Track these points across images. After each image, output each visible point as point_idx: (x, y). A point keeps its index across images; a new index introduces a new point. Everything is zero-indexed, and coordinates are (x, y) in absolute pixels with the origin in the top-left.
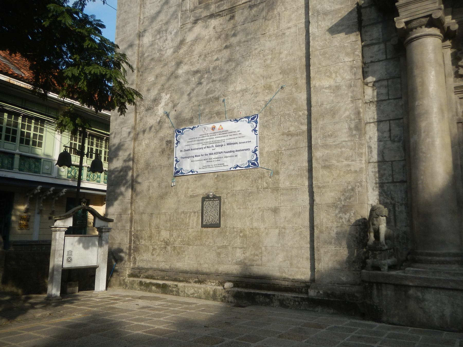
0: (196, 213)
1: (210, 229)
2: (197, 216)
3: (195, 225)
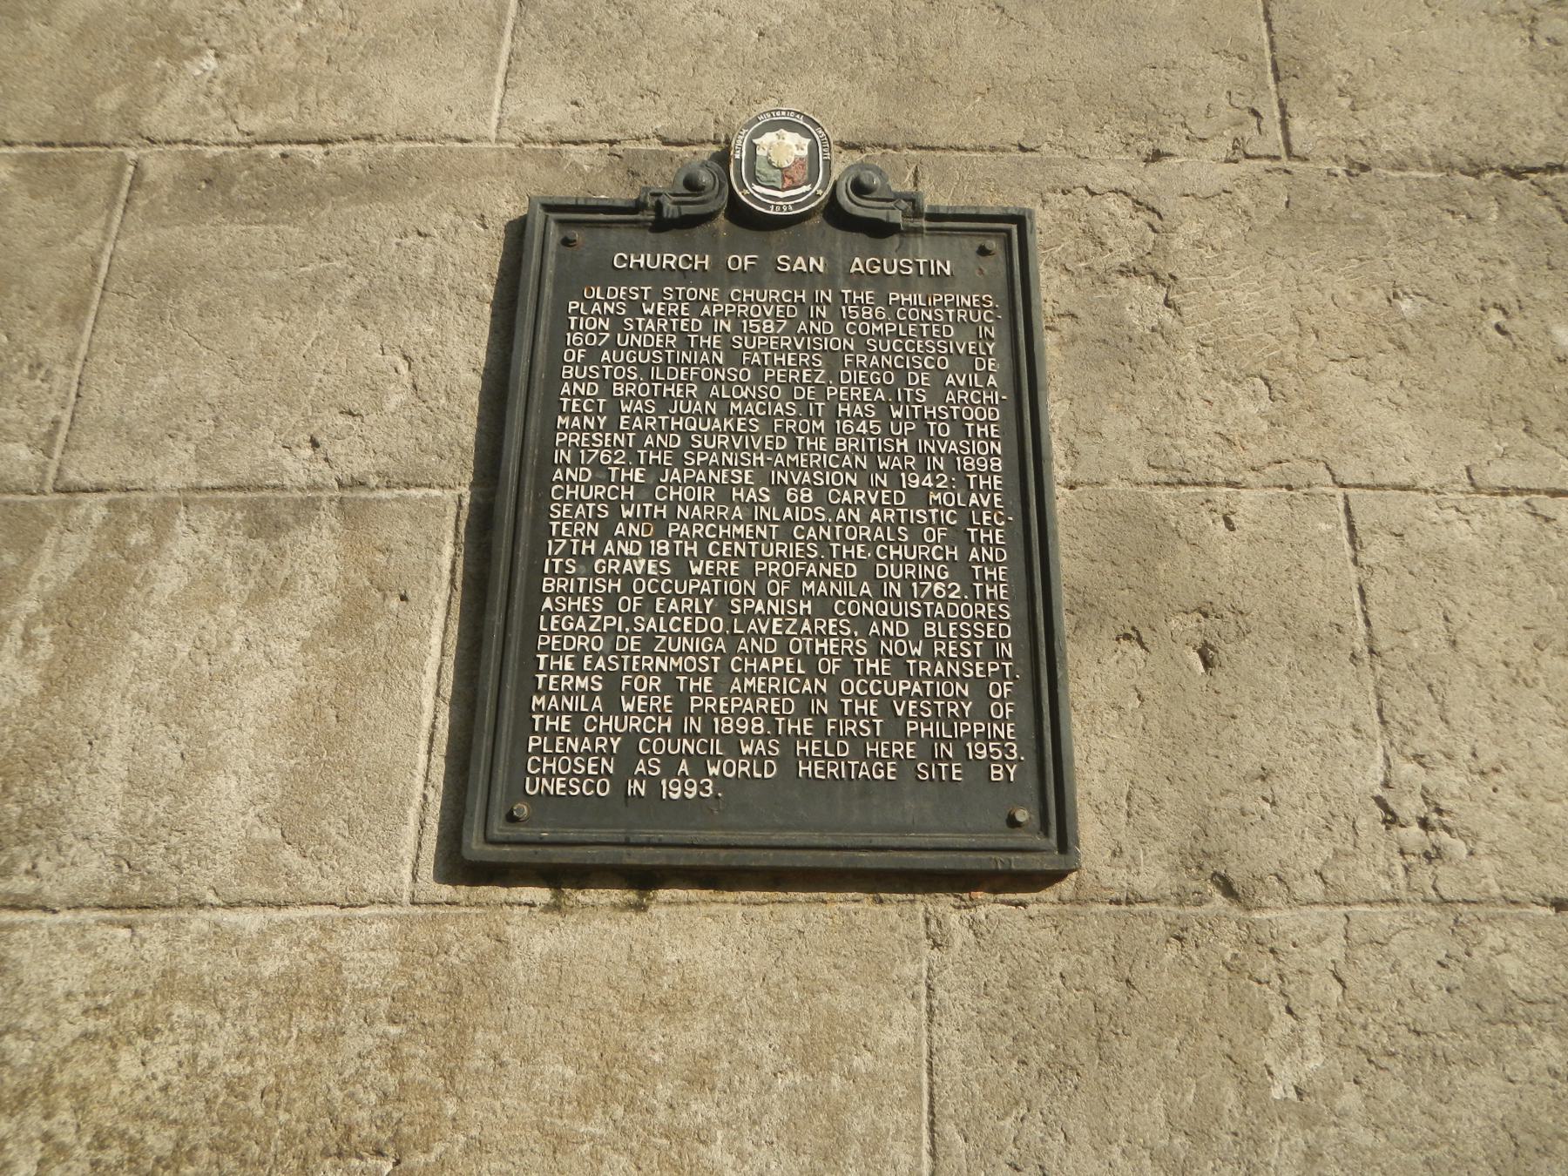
0: (319, 548)
1: (703, 935)
2: (314, 602)
3: (231, 806)
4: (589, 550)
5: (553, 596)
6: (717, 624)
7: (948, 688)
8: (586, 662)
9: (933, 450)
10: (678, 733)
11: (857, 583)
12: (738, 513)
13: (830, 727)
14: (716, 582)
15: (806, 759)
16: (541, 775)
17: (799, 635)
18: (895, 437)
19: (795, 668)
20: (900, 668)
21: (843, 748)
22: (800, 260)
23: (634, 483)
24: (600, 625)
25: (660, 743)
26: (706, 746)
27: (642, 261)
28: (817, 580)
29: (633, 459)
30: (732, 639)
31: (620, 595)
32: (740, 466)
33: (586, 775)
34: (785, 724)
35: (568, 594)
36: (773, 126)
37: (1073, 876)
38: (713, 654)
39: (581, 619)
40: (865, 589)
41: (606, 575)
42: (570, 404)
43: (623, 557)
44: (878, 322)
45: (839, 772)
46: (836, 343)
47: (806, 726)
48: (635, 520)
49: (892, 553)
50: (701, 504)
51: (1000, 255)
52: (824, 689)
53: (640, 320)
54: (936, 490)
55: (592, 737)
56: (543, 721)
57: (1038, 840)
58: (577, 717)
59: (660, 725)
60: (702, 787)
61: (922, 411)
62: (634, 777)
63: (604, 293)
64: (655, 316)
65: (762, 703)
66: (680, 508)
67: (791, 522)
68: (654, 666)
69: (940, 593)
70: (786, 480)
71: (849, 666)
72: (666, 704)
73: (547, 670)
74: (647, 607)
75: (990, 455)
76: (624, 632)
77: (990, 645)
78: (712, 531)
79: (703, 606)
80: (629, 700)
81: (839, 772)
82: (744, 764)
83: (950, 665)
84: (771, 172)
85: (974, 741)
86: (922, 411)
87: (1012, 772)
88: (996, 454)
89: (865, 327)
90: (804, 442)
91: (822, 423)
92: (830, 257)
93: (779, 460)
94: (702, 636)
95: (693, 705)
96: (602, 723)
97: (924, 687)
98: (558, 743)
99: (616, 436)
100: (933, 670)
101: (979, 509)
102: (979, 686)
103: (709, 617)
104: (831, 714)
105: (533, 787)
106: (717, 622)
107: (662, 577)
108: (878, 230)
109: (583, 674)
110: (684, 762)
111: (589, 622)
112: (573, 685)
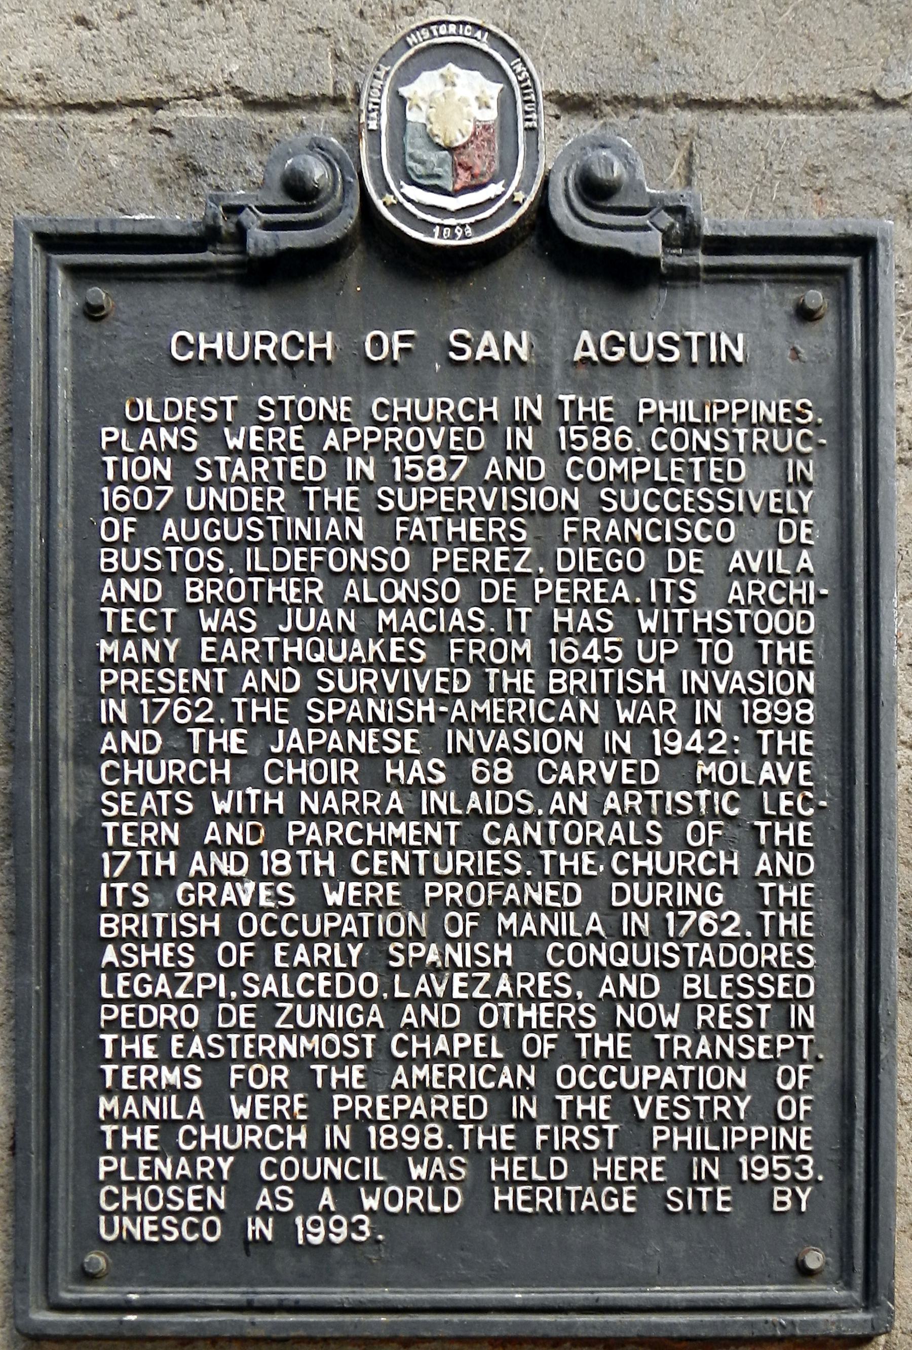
4: (166, 868)
5: (117, 941)
8: (175, 1045)
9: (705, 688)
10: (317, 1149)
12: (396, 802)
13: (540, 1138)
14: (366, 916)
15: (505, 1183)
17: (494, 1000)
18: (643, 666)
19: (486, 1049)
20: (645, 1046)
21: (559, 1167)
22: (488, 337)
24: (192, 987)
25: (290, 1165)
26: (357, 1168)
27: (218, 346)
28: (521, 911)
29: (224, 715)
30: (393, 1006)
31: (219, 940)
33: (185, 1212)
34: (473, 1133)
35: (139, 940)
37: (882, 1339)
38: (363, 1029)
39: (163, 978)
40: (595, 923)
41: (195, 908)
42: (117, 617)
43: (220, 879)
45: (553, 1202)
47: (504, 1137)
48: (234, 817)
51: (829, 321)
52: (531, 1080)
53: (223, 460)
54: (710, 758)
55: (191, 1156)
56: (117, 1134)
57: (835, 1293)
58: (167, 1127)
59: (290, 1138)
60: (354, 1227)
61: (688, 618)
62: (256, 1213)
63: (158, 410)
64: (247, 453)
65: (439, 1102)
66: (304, 797)
67: (479, 817)
68: (276, 1050)
69: (708, 927)
70: (470, 746)
71: (569, 1045)
72: (297, 1106)
73: (117, 1058)
75: (796, 696)
76: (228, 999)
78: (357, 832)
80: (241, 1102)
81: (553, 1202)
82: (415, 1193)
83: (719, 1040)
84: (434, 157)
85: (751, 1153)
86: (688, 618)
88: (806, 694)
89: (597, 466)
90: (498, 677)
91: (527, 644)
92: (538, 331)
93: (458, 710)
94: (346, 1002)
95: (337, 1108)
97: (679, 1074)
98: (142, 1167)
99: (196, 674)
100: (693, 1050)
101: (774, 787)
104: (541, 1119)
105: (110, 1230)
106: (369, 981)
107: (283, 910)
108: (624, 276)
110: (327, 1191)
111: (175, 983)
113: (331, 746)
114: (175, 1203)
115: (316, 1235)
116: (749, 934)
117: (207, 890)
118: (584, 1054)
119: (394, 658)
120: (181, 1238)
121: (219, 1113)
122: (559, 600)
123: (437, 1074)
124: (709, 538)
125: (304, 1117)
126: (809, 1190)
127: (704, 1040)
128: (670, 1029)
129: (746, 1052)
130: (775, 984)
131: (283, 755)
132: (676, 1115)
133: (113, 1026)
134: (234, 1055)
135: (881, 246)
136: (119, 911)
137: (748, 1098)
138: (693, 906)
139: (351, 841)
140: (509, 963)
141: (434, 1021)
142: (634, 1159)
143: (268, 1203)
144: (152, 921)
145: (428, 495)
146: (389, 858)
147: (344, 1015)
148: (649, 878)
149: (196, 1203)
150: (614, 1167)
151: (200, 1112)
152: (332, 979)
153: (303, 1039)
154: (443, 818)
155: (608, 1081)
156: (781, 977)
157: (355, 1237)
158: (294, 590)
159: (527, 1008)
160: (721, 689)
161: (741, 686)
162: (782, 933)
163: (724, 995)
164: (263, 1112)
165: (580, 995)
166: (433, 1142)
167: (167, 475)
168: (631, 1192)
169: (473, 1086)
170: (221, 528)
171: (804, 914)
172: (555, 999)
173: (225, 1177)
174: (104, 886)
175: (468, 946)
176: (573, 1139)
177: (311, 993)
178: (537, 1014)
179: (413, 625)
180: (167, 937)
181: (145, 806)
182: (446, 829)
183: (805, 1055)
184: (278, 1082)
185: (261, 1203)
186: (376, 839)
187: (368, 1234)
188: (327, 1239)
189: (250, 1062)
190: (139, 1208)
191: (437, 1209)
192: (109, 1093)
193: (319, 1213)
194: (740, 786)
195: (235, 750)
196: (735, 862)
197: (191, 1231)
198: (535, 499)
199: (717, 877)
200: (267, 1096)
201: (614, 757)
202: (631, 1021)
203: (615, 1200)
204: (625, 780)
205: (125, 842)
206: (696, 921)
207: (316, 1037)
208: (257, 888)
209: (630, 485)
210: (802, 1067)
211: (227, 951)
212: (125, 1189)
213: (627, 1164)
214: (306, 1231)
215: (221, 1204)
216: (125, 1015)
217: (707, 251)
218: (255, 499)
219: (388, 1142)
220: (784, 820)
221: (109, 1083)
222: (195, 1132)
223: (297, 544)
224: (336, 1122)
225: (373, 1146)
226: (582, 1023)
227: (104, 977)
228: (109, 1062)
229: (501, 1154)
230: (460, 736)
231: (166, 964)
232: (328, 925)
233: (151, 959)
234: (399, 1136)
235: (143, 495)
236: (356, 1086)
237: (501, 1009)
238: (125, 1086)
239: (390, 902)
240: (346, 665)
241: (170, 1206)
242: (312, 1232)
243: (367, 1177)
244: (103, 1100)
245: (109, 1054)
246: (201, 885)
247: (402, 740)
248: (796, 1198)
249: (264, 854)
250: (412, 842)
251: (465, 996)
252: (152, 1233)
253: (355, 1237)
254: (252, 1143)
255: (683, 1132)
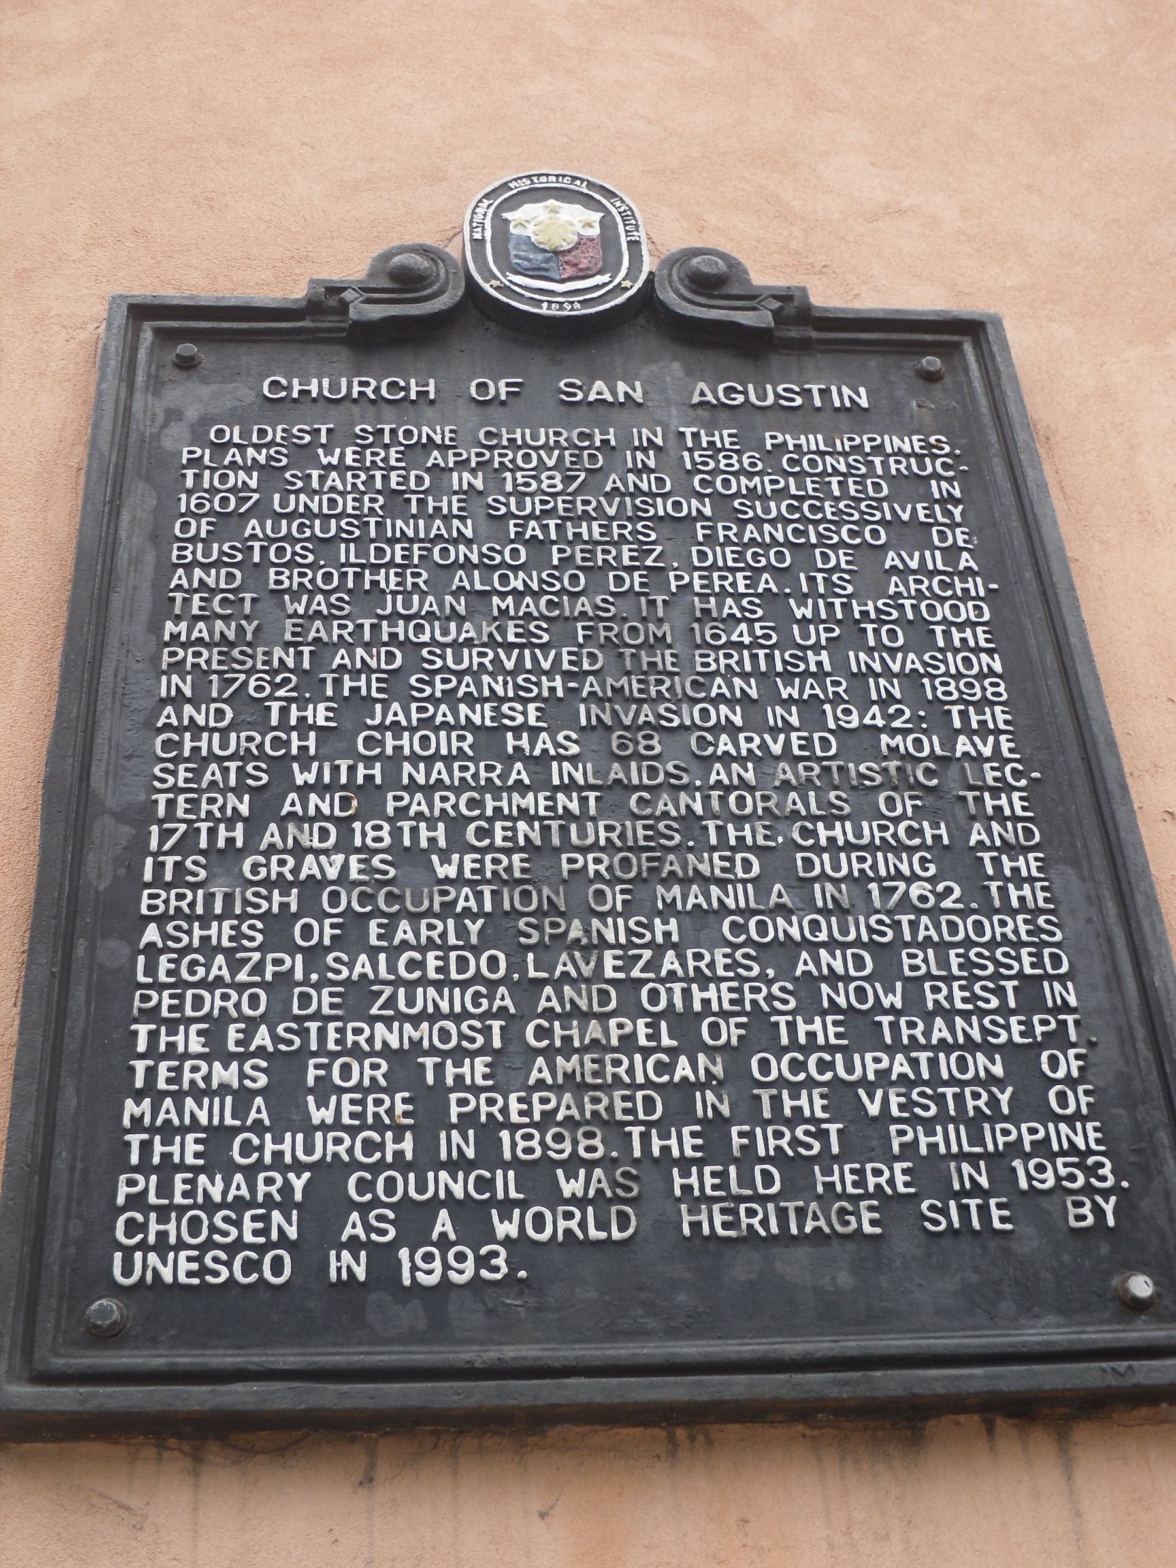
4: (230, 841)
5: (162, 920)
6: (493, 962)
7: (962, 1065)
9: (877, 667)
10: (426, 1161)
11: (761, 884)
12: (519, 773)
13: (736, 1141)
15: (696, 1201)
16: (143, 1246)
18: (804, 648)
19: (654, 1036)
22: (599, 385)
23: (314, 727)
24: (258, 969)
31: (296, 916)
32: (518, 698)
36: (535, 194)
38: (488, 1015)
39: (220, 959)
41: (266, 882)
43: (299, 851)
44: (750, 475)
46: (677, 505)
47: (688, 1142)
48: (319, 788)
49: (823, 834)
50: (448, 760)
52: (718, 1070)
54: (894, 732)
55: (249, 1173)
56: (146, 1146)
59: (390, 1147)
60: (483, 1262)
62: (341, 1246)
64: (341, 468)
66: (407, 767)
68: (370, 1040)
69: (923, 899)
72: (400, 1108)
74: (351, 934)
75: (981, 676)
76: (306, 982)
77: (1030, 986)
79: (462, 932)
80: (322, 1103)
81: (765, 1223)
82: (568, 1216)
83: (959, 1022)
87: (1109, 1208)
89: (727, 483)
91: (666, 627)
94: (464, 985)
96: (269, 1147)
97: (914, 1063)
98: (179, 1187)
99: (278, 652)
100: (927, 1033)
102: (1020, 1057)
103: (477, 951)
105: (127, 1271)
109: (227, 1059)
110: (444, 1214)
111: (235, 965)
112: (207, 1078)
113: (439, 719)
114: (225, 1234)
115: (430, 1272)
116: (974, 905)
117: (282, 863)
118: (785, 1041)
119: (511, 638)
120: (231, 1279)
121: (288, 1115)
122: (697, 589)
123: (589, 1066)
124: (858, 541)
125: (410, 1121)
126: (1113, 1199)
127: (939, 1022)
128: (892, 1010)
129: (997, 1035)
130: (1018, 959)
131: (381, 728)
132: (917, 1110)
133: (151, 1015)
134: (314, 1047)
135: (990, 329)
136: (168, 886)
137: (1010, 1090)
138: (899, 875)
139: (465, 811)
140: (675, 938)
141: (583, 1004)
142: (869, 1167)
143: (360, 1231)
144: (209, 898)
145: (543, 502)
146: (514, 829)
147: (461, 1000)
148: (842, 849)
149: (256, 1233)
150: (844, 1177)
151: (264, 1115)
152: (445, 958)
153: (407, 1027)
154: (581, 789)
155: (821, 1072)
156: (1024, 952)
157: (484, 1273)
158: (393, 579)
159: (704, 988)
160: (896, 668)
161: (918, 666)
162: (1015, 903)
163: (955, 971)
164: (352, 1115)
165: (771, 973)
166: (591, 1149)
167: (253, 484)
168: (871, 1209)
169: (640, 1079)
170: (311, 527)
171: (1038, 884)
172: (739, 977)
173: (298, 1197)
174: (149, 861)
175: (620, 921)
176: (784, 1143)
177: (417, 974)
178: (719, 995)
179: (532, 609)
180: (227, 913)
181: (208, 776)
182: (584, 801)
183: (1073, 1038)
184: (373, 1079)
185: (348, 1232)
186: (498, 810)
187: (504, 1270)
188: (444, 1275)
189: (334, 1055)
190: (172, 1240)
191: (603, 1235)
192: (139, 1096)
193: (433, 1244)
194: (933, 756)
195: (321, 722)
196: (943, 831)
197: (246, 1274)
198: (662, 507)
199: (923, 847)
200: (358, 1096)
201: (780, 730)
202: (841, 1001)
203: (852, 1219)
204: (796, 752)
205: (180, 813)
206: (906, 893)
207: (425, 1025)
208: (346, 861)
209: (764, 498)
210: (1071, 1052)
211: (307, 931)
212: (153, 1216)
213: (861, 1173)
214: (414, 1268)
215: (292, 1232)
216: (166, 1002)
217: (817, 328)
218: (350, 504)
219: (529, 1151)
220: (995, 793)
221: (139, 1083)
222: (256, 1141)
223: (398, 541)
224: (454, 1126)
225: (507, 1155)
226: (777, 1004)
227: (141, 959)
228: (142, 1057)
229: (685, 1164)
230: (594, 710)
231: (225, 943)
232: (437, 899)
233: (205, 940)
234: (542, 1143)
235: (225, 501)
236: (480, 1081)
237: (670, 991)
238: (162, 1085)
239: (517, 874)
240: (455, 644)
241: (217, 1237)
242: (420, 1269)
243: (500, 1195)
244: (129, 1103)
245: (142, 1047)
246: (274, 859)
247: (524, 713)
248: (1098, 1211)
249: (357, 825)
250: (542, 812)
251: (621, 975)
252: (190, 1274)
253: (484, 1273)
254: (336, 1155)
255: (931, 1133)
